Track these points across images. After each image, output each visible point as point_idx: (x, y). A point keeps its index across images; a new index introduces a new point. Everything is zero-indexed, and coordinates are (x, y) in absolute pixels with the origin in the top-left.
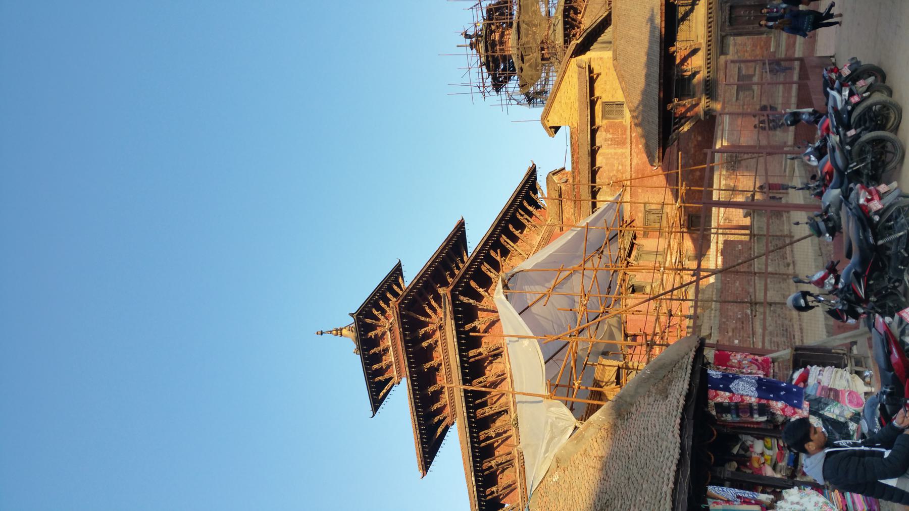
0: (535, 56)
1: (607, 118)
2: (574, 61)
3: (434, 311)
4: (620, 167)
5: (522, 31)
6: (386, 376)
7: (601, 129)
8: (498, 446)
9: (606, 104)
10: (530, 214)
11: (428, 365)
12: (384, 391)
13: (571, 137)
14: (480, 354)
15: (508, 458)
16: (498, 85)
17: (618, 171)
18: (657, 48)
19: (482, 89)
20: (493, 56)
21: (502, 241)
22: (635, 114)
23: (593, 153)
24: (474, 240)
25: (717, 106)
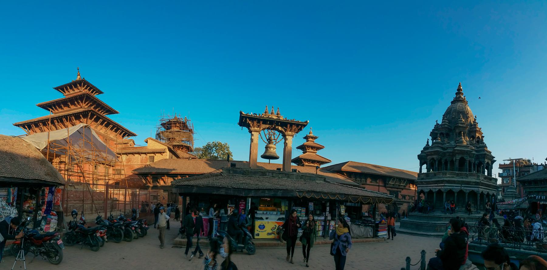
0: (171, 136)
1: (149, 157)
2: (167, 147)
3: (87, 105)
4: (134, 162)
5: (178, 133)
6: (66, 91)
7: (146, 156)
8: (47, 128)
9: (154, 157)
10: (120, 134)
11: (70, 104)
12: (61, 91)
13: (144, 147)
14: (73, 120)
15: (43, 131)
16: (163, 125)
17: (133, 161)
18: (166, 171)
19: (162, 120)
20: (172, 123)
21: (110, 125)
22: (148, 165)
23: (139, 153)
24: (111, 117)
25: (150, 189)
